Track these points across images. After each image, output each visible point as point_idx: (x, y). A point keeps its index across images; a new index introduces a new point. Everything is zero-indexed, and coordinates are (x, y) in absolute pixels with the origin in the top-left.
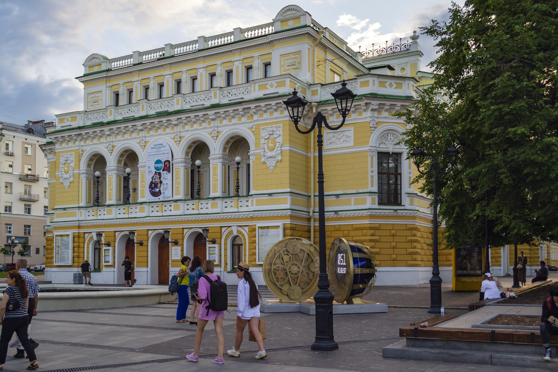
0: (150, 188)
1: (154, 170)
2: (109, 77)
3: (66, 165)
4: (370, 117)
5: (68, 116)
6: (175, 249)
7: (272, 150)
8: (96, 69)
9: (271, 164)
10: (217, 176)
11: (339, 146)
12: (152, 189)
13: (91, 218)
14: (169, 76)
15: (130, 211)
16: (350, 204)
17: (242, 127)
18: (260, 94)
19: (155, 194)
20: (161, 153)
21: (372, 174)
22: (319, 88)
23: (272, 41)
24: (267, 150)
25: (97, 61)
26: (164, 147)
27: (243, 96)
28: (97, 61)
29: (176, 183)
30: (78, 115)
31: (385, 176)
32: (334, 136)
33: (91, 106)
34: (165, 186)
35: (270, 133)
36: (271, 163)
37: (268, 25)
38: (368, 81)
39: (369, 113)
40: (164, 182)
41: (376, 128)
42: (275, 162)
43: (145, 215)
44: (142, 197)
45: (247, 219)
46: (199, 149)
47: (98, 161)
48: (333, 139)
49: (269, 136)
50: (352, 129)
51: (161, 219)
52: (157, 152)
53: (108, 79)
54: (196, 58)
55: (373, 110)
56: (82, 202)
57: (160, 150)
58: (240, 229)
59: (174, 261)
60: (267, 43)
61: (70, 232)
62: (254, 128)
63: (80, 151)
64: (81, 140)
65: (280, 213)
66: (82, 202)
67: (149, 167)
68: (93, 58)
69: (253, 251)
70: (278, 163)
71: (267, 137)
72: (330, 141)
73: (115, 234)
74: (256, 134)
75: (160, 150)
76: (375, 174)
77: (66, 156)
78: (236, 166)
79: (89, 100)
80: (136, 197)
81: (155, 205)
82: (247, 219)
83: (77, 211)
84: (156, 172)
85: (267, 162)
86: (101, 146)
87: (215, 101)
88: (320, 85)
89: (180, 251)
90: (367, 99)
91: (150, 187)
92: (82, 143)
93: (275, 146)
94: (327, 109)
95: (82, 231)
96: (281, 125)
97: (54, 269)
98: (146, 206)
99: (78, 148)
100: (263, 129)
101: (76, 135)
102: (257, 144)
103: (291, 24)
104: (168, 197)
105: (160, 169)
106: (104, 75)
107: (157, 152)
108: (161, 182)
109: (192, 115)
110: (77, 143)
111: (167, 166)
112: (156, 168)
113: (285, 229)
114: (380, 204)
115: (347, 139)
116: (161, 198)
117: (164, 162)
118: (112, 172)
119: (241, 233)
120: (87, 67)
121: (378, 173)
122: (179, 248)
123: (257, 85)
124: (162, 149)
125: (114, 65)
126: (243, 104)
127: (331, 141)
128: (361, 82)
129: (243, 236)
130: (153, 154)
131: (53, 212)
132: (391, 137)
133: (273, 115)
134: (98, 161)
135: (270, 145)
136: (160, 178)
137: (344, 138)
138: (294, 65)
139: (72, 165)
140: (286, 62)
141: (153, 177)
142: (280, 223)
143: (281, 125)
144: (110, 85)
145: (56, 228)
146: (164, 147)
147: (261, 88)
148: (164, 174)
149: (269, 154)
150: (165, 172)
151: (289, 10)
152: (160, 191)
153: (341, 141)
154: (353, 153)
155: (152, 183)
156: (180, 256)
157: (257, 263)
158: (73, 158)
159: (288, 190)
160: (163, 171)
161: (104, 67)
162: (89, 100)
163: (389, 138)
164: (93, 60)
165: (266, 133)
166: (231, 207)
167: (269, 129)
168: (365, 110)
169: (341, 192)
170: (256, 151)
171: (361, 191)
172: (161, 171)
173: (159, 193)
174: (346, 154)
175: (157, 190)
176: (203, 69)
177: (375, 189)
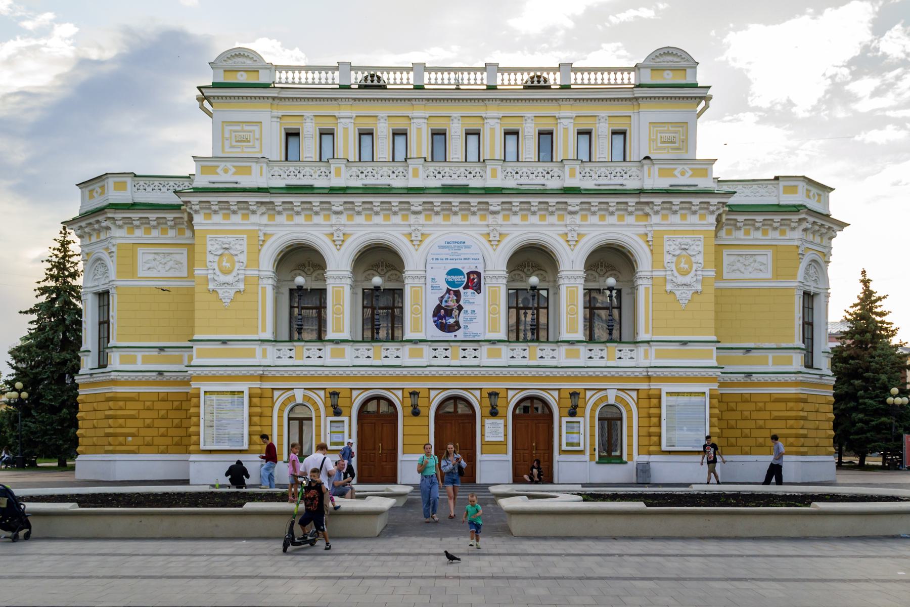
0: (434, 315)
1: (445, 287)
2: (281, 99)
4: (801, 239)
5: (228, 164)
7: (685, 273)
8: (242, 78)
9: (684, 295)
10: (499, 306)
11: (747, 276)
12: (441, 318)
13: (286, 361)
14: (423, 120)
17: (626, 230)
18: (664, 183)
19: (444, 327)
20: (462, 257)
23: (637, 99)
25: (249, 62)
26: (468, 247)
27: (624, 182)
28: (249, 62)
29: (487, 313)
32: (755, 261)
33: (232, 147)
34: (470, 315)
35: (683, 247)
36: (683, 295)
37: (629, 70)
38: (796, 186)
39: (797, 234)
40: (465, 307)
43: (419, 362)
44: (416, 330)
45: (636, 379)
46: (532, 259)
48: (739, 265)
51: (534, 371)
52: (453, 254)
53: (277, 101)
55: (805, 230)
56: (264, 330)
57: (459, 252)
58: (621, 394)
60: (630, 99)
61: (244, 387)
62: (650, 235)
63: (261, 234)
64: (263, 214)
65: (704, 372)
66: (264, 330)
67: (433, 279)
68: (239, 55)
70: (695, 295)
74: (653, 245)
75: (459, 252)
77: (225, 240)
80: (635, 332)
81: (441, 347)
82: (636, 379)
83: (257, 347)
84: (448, 291)
85: (678, 293)
86: (314, 231)
87: (570, 183)
89: (502, 426)
90: (807, 214)
91: (436, 313)
92: (265, 220)
93: (691, 268)
94: (736, 220)
96: (702, 236)
97: (193, 457)
98: (426, 349)
99: (257, 228)
101: (258, 202)
102: (656, 262)
103: (669, 78)
104: (476, 335)
105: (459, 286)
107: (453, 254)
108: (460, 308)
109: (516, 200)
110: (254, 219)
111: (474, 282)
112: (448, 282)
113: (711, 397)
115: (762, 268)
116: (460, 335)
117: (468, 274)
118: (344, 281)
119: (622, 400)
120: (222, 71)
124: (463, 251)
125: (282, 77)
126: (642, 195)
127: (735, 268)
128: (784, 186)
129: (627, 405)
130: (444, 257)
131: (190, 344)
133: (686, 219)
134: (300, 257)
135: (682, 265)
136: (458, 301)
137: (756, 265)
138: (674, 143)
139: (243, 258)
140: (659, 135)
141: (442, 297)
142: (705, 388)
143: (702, 236)
144: (280, 115)
145: (200, 378)
146: (468, 247)
147: (663, 173)
148: (467, 295)
150: (469, 291)
151: (668, 54)
152: (457, 323)
154: (770, 288)
155: (439, 307)
156: (502, 435)
158: (240, 246)
160: (465, 288)
162: (227, 135)
166: (604, 357)
167: (679, 240)
169: (752, 345)
171: (784, 345)
172: (461, 289)
173: (456, 326)
174: (759, 288)
175: (452, 321)
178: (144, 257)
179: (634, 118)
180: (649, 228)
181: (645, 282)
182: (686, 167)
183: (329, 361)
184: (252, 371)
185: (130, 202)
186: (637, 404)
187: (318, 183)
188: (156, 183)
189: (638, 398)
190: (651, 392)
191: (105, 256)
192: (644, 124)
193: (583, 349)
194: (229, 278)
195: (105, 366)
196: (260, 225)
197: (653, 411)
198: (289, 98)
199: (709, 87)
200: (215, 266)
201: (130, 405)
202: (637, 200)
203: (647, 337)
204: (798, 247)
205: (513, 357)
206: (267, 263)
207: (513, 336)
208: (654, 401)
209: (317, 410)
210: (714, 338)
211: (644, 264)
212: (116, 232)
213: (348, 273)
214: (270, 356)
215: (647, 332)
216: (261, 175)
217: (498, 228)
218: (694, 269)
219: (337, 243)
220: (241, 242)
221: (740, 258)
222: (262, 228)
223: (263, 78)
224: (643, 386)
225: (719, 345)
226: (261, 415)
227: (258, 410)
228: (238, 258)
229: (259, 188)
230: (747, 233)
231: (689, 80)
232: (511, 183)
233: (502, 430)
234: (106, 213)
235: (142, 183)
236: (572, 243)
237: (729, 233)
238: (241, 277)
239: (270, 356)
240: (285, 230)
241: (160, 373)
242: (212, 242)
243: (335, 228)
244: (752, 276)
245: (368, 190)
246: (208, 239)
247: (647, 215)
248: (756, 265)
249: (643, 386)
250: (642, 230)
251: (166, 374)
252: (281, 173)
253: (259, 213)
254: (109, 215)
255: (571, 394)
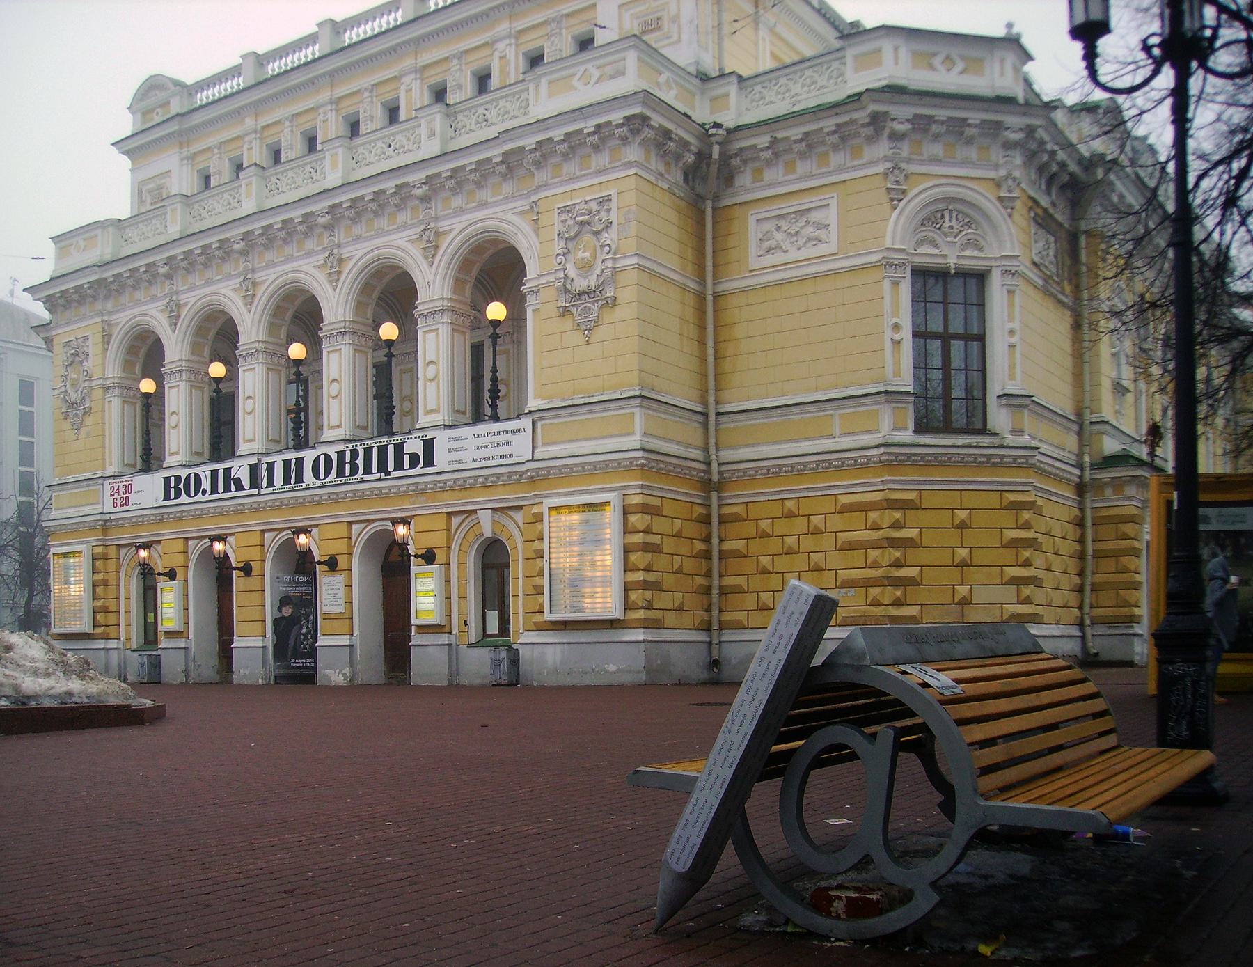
4: (886, 158)
6: (329, 584)
11: (793, 255)
17: (502, 215)
21: (897, 337)
22: (733, 89)
24: (572, 272)
30: (99, 232)
31: (936, 345)
38: (878, 51)
41: (904, 192)
42: (596, 308)
47: (146, 353)
49: (577, 228)
50: (833, 204)
58: (499, 517)
59: (327, 617)
64: (107, 298)
69: (537, 581)
71: (572, 234)
72: (767, 244)
73: (186, 545)
76: (906, 334)
78: (491, 330)
88: (734, 79)
89: (341, 586)
92: (109, 306)
106: (173, 127)
113: (626, 512)
114: (920, 429)
121: (916, 335)
122: (339, 578)
127: (772, 243)
132: (954, 223)
134: (146, 353)
137: (809, 230)
149: (580, 284)
153: (800, 243)
156: (342, 601)
157: (548, 616)
159: (638, 393)
161: (176, 107)
163: (947, 224)
164: (153, 91)
165: (571, 222)
168: (870, 140)
176: (413, 76)
177: (906, 382)
182: (590, 67)
221: (782, 223)
226: (105, 584)
227: (101, 576)
230: (790, 168)
233: (341, 593)
237: (758, 173)
244: (804, 254)
248: (809, 230)
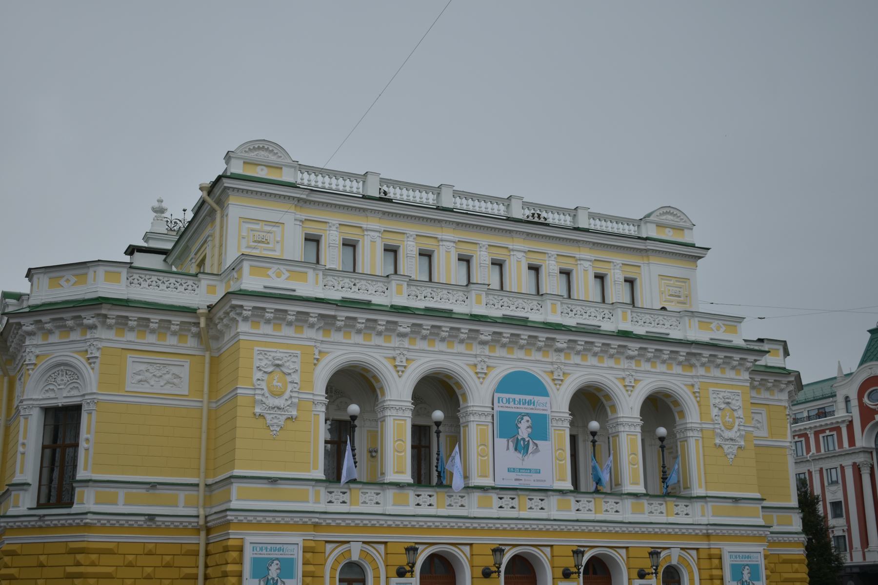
2: (311, 202)
3: (277, 376)
7: (730, 428)
14: (452, 244)
15: (605, 507)
16: (115, 503)
23: (647, 250)
47: (354, 385)
54: (440, 221)
62: (696, 386)
63: (317, 352)
66: (316, 468)
77: (278, 355)
79: (244, 234)
83: (310, 488)
92: (320, 336)
95: (323, 536)
99: (313, 344)
100: (714, 392)
101: (320, 315)
115: (758, 425)
123: (696, 319)
125: (306, 179)
134: (354, 385)
138: (679, 297)
167: (722, 394)
170: (704, 426)
178: (133, 366)
179: (644, 269)
180: (695, 380)
181: (696, 434)
183: (391, 509)
184: (306, 518)
185: (125, 297)
186: (698, 565)
187: (377, 300)
188: (154, 278)
189: (699, 559)
190: (713, 552)
191: (79, 361)
192: (653, 275)
193: (411, 493)
194: (277, 402)
195: (70, 504)
196: (316, 341)
197: (716, 572)
198: (315, 202)
199: (708, 249)
200: (264, 385)
201: (105, 559)
202: (688, 350)
203: (701, 492)
204: (785, 407)
205: (501, 507)
206: (320, 389)
207: (656, 487)
208: (716, 562)
209: (376, 569)
210: (758, 495)
211: (693, 417)
212: (102, 333)
213: (410, 404)
214: (317, 501)
215: (700, 487)
216: (317, 283)
217: (562, 367)
218: (737, 424)
219: (399, 368)
220: (294, 359)
222: (318, 345)
223: (287, 176)
224: (703, 544)
225: (765, 504)
228: (284, 378)
229: (316, 298)
231: (687, 239)
232: (570, 321)
234: (101, 308)
235: (136, 276)
236: (629, 388)
238: (296, 400)
239: (317, 501)
240: (342, 351)
241: (151, 517)
242: (261, 357)
243: (398, 352)
245: (430, 313)
246: (256, 352)
247: (692, 366)
249: (703, 544)
250: (690, 381)
251: (157, 519)
252: (336, 284)
253: (317, 327)
254: (104, 312)
255: (651, 554)
